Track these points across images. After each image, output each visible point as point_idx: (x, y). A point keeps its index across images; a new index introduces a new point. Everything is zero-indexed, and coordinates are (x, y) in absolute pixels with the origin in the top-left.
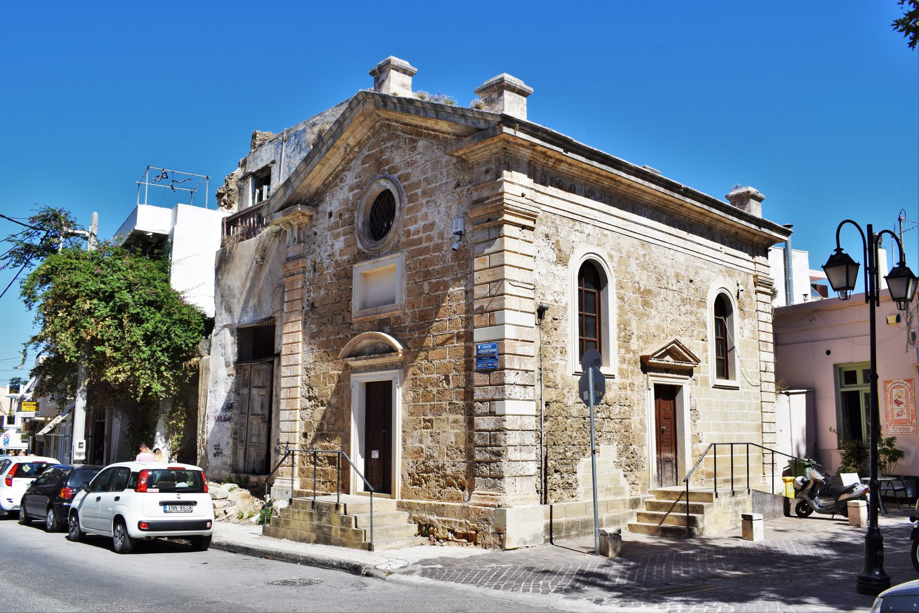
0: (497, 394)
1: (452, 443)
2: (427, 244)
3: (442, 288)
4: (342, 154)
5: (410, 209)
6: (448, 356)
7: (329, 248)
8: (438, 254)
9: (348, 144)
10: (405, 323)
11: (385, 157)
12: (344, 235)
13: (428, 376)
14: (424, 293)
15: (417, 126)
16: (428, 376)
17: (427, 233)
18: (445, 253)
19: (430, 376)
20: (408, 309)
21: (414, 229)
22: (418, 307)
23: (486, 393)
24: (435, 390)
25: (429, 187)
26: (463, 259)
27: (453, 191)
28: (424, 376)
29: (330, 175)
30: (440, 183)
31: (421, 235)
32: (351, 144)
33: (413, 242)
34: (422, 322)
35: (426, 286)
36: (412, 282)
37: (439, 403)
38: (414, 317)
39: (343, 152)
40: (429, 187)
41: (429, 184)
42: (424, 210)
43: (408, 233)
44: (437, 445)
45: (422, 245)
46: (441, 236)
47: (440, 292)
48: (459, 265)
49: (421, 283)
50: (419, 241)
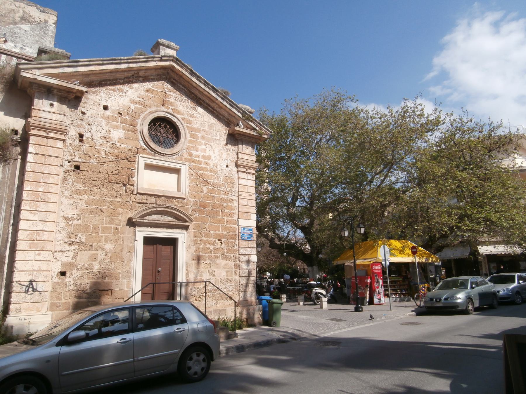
0: (252, 252)
1: (224, 276)
2: (205, 166)
3: (216, 193)
4: (129, 75)
5: (190, 142)
6: (221, 230)
7: (104, 132)
8: (214, 174)
9: (138, 73)
10: (188, 205)
11: (170, 100)
12: (124, 129)
13: (206, 239)
14: (203, 192)
15: (200, 98)
16: (206, 239)
17: (206, 160)
18: (218, 176)
19: (208, 239)
20: (191, 198)
21: (195, 154)
22: (198, 199)
23: (247, 251)
24: (212, 247)
25: (207, 136)
26: (230, 182)
27: (224, 146)
28: (203, 238)
29: (109, 80)
30: (214, 138)
31: (200, 159)
32: (140, 74)
33: (194, 161)
34: (202, 208)
35: (205, 189)
36: (194, 183)
37: (215, 254)
38: (195, 204)
39: (131, 75)
40: (206, 135)
41: (207, 134)
42: (203, 147)
43: (191, 155)
44: (213, 277)
45: (201, 165)
46: (216, 165)
47: (215, 195)
48: (228, 185)
49: (201, 186)
50: (200, 163)
